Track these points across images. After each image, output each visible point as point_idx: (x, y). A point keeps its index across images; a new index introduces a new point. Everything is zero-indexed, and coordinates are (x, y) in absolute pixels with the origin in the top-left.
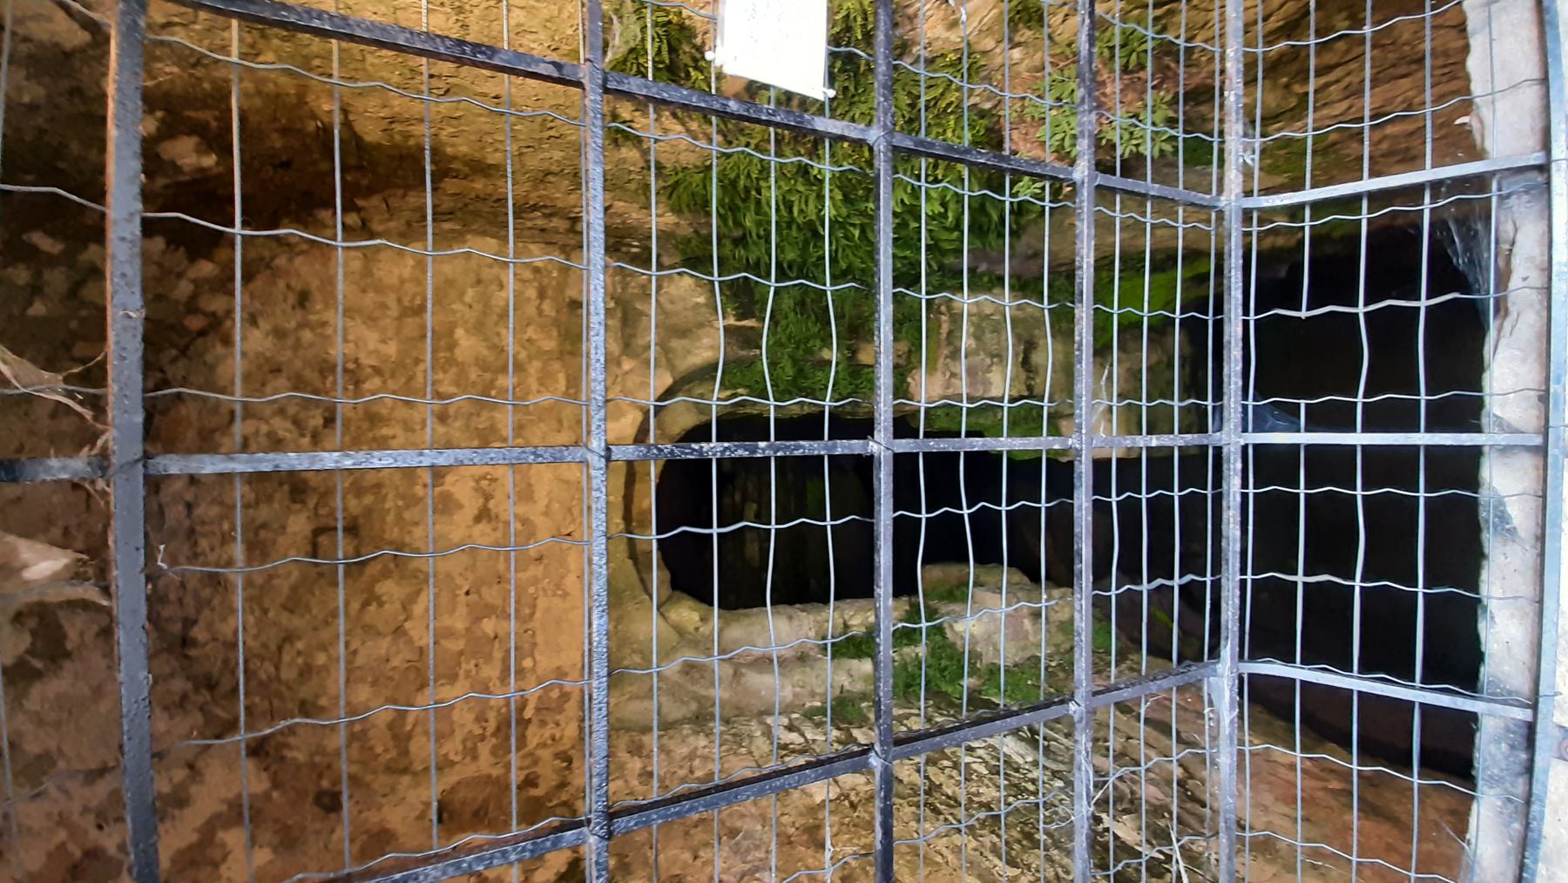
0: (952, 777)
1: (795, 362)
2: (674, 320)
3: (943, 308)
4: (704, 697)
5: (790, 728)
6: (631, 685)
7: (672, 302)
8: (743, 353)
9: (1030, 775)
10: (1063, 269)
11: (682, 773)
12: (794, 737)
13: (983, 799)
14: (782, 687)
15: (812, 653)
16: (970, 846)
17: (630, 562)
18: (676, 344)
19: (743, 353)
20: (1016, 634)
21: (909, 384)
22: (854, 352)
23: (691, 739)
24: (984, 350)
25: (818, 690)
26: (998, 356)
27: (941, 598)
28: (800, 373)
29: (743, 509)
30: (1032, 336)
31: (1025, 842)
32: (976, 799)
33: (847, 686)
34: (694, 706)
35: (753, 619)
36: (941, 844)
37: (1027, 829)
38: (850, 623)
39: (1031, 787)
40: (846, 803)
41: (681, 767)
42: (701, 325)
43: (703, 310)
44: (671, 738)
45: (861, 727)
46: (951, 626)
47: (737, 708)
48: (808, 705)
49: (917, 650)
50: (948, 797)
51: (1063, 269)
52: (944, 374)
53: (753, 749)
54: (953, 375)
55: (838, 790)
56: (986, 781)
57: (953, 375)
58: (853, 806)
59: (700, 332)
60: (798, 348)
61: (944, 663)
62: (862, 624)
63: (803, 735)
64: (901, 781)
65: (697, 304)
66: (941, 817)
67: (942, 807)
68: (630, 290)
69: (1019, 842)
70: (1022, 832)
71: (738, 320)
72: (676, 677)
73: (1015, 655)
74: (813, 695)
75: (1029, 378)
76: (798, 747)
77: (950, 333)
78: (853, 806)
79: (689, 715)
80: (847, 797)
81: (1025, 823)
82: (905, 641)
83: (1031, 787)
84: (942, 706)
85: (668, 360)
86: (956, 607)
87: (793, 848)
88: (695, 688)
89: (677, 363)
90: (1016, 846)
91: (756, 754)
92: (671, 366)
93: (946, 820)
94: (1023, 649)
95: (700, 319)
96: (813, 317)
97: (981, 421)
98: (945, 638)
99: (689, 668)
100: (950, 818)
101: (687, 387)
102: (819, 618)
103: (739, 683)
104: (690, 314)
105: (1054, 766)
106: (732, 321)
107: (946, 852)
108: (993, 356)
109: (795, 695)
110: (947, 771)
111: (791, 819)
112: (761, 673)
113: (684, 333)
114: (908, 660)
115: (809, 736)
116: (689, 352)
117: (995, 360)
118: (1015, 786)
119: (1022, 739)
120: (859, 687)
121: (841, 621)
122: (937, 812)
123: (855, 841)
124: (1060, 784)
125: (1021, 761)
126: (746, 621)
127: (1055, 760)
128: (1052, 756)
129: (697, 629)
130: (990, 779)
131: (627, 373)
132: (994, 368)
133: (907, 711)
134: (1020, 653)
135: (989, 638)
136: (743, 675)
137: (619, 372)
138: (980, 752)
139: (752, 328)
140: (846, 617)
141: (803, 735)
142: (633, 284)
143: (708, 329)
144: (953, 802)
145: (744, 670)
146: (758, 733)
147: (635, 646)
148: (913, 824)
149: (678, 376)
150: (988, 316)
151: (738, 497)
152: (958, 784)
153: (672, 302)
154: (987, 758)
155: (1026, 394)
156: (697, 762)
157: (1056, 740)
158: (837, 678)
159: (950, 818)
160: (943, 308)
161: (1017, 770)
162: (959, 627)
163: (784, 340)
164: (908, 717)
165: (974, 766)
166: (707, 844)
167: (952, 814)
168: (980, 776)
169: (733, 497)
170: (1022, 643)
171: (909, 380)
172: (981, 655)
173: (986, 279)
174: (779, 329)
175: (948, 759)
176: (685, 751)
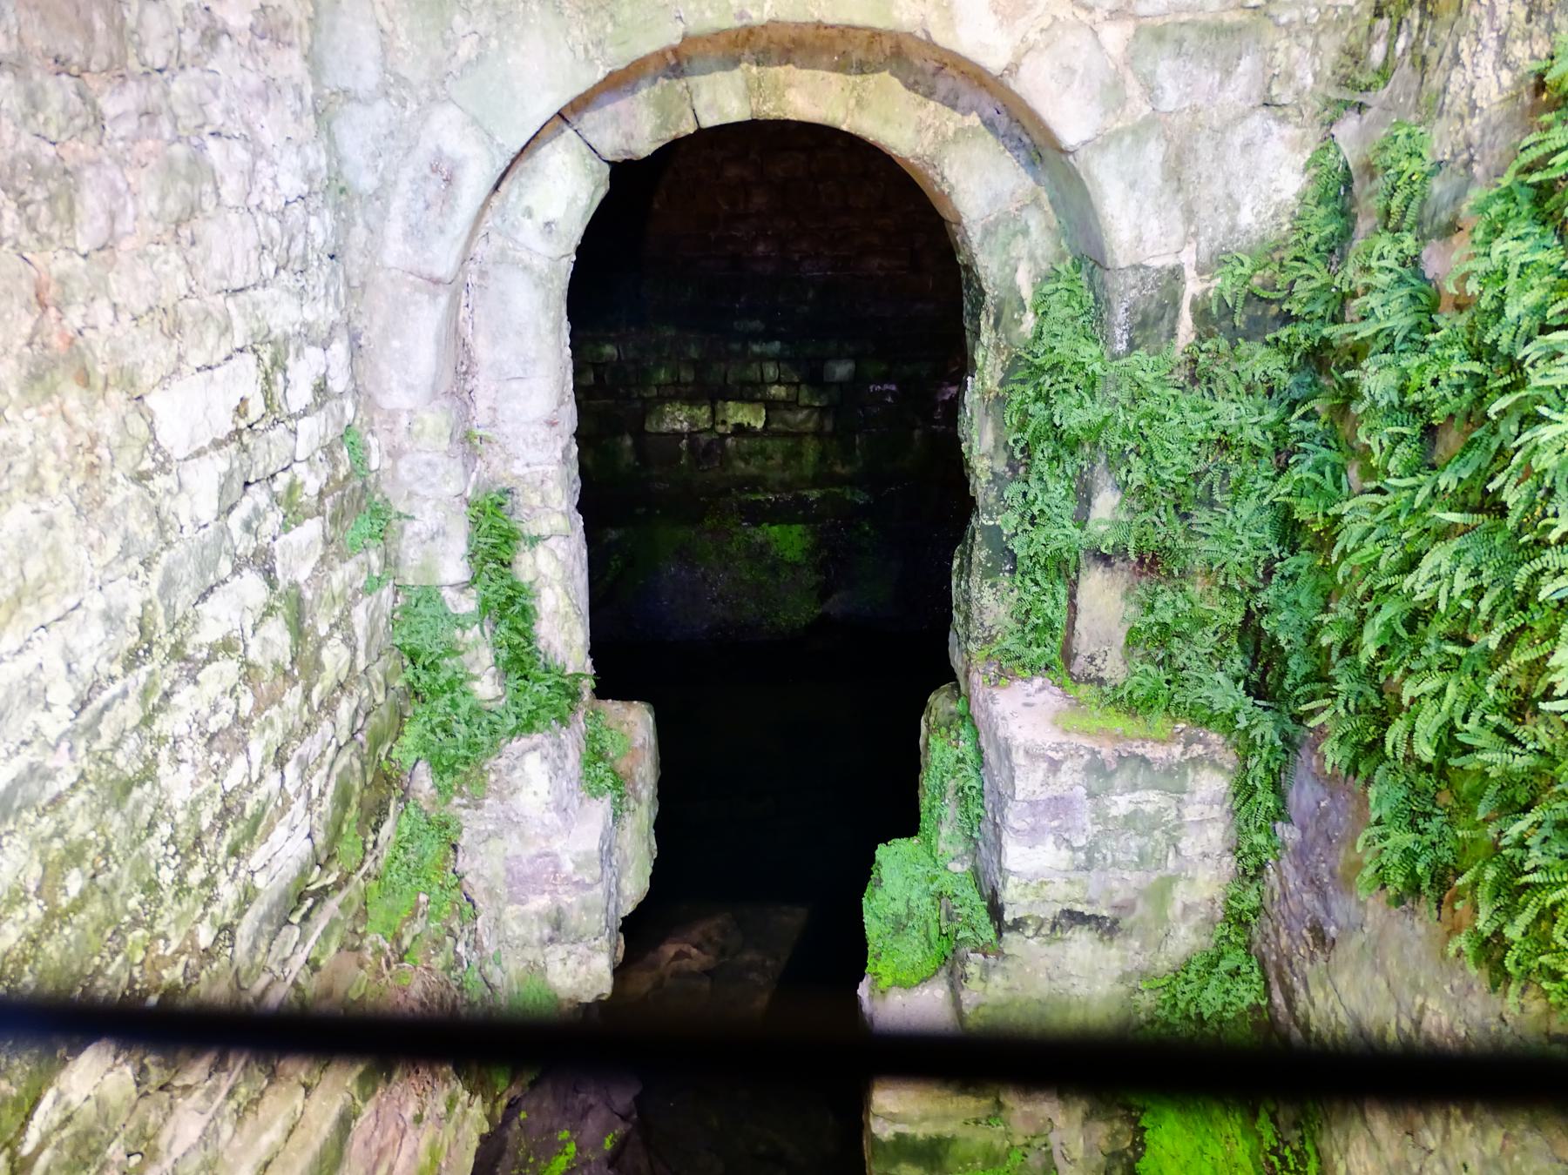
0: (215, 710)
1: (1095, 431)
2: (1205, 148)
3: (1198, 749)
4: (386, 209)
5: (321, 388)
6: (410, 33)
7: (1247, 145)
8: (1121, 316)
9: (222, 878)
10: (1278, 999)
11: (216, 112)
12: (300, 396)
13: (164, 770)
14: (410, 387)
15: (480, 464)
16: (44, 720)
17: (668, 35)
18: (1154, 152)
19: (1121, 316)
20: (519, 883)
21: (1028, 680)
22: (1105, 559)
23: (296, 161)
24: (1106, 833)
25: (403, 465)
26: (1090, 860)
27: (591, 738)
28: (1067, 444)
29: (751, 400)
30: (1128, 934)
31: (57, 844)
32: (164, 754)
33: (411, 528)
34: (367, 182)
35: (551, 340)
36: (48, 651)
37: (91, 854)
38: (540, 548)
39: (195, 876)
40: (148, 464)
41: (228, 111)
42: (1189, 214)
43: (1224, 220)
44: (297, 118)
45: (328, 542)
46: (534, 749)
47: (363, 285)
48: (373, 442)
49: (487, 679)
50: (167, 695)
51: (1278, 999)
52: (1058, 747)
53: (273, 291)
54: (1055, 766)
55: (179, 453)
56: (208, 782)
57: (1055, 766)
58: (141, 478)
59: (1176, 213)
60: (1126, 434)
61: (462, 730)
62: (538, 574)
63: (305, 413)
64: (203, 597)
65: (1238, 208)
66: (117, 669)
67: (141, 674)
68: (1282, 44)
69: (59, 833)
70: (85, 843)
71: (1194, 304)
72: (427, 145)
73: (479, 876)
74: (395, 453)
75: (1041, 924)
76: (278, 390)
77: (1144, 760)
78: (141, 478)
79: (347, 171)
80: (163, 468)
81: (106, 851)
82: (504, 654)
83: (195, 876)
84: (373, 719)
85: (1118, 136)
86: (572, 762)
87: (27, 307)
88: (404, 186)
89: (1111, 157)
90: (47, 825)
91: (259, 294)
92: (1102, 142)
93: (112, 679)
94: (490, 892)
95: (1204, 212)
96: (1197, 468)
97: (945, 831)
98: (512, 733)
99: (447, 175)
100: (115, 688)
101: (1045, 197)
102: (550, 484)
103: (417, 289)
104: (1217, 189)
105: (245, 929)
106: (1193, 287)
107: (27, 662)
108: (1091, 850)
109: (393, 416)
110: (228, 703)
111: (104, 326)
112: (438, 342)
113: (1176, 172)
114: (466, 658)
115: (304, 425)
116: (1132, 185)
117: (1082, 856)
118: (198, 842)
119: (304, 873)
120: (412, 554)
121: (545, 531)
122: (132, 660)
123: (51, 459)
124: (205, 937)
125: (255, 862)
126: (546, 324)
127: (259, 932)
128: (267, 928)
129: (529, 213)
130: (212, 793)
131: (1095, 34)
132: (1065, 853)
133: (362, 645)
134: (481, 884)
135: (512, 822)
136: (434, 296)
137: (1099, 15)
138: (273, 780)
139: (1173, 333)
140: (552, 543)
141: (305, 413)
142: (1296, 52)
143: (1180, 229)
144: (157, 704)
145: (443, 300)
146: (309, 316)
147: (494, 43)
148: (96, 603)
149: (1077, 162)
150: (1174, 843)
151: (778, 391)
152: (199, 722)
153: (1247, 145)
154: (260, 793)
155: (1008, 917)
156: (240, 154)
157: (303, 939)
158: (428, 506)
159: (115, 688)
160: (1198, 749)
161: (234, 851)
162: (533, 763)
163: (1148, 405)
164: (349, 641)
165: (240, 762)
166: (34, 102)
167: (125, 693)
168: (216, 771)
169: (779, 382)
170: (502, 890)
171: (1038, 682)
172: (478, 807)
173: (1260, 839)
174: (1175, 392)
175: (258, 709)
176: (268, 136)
